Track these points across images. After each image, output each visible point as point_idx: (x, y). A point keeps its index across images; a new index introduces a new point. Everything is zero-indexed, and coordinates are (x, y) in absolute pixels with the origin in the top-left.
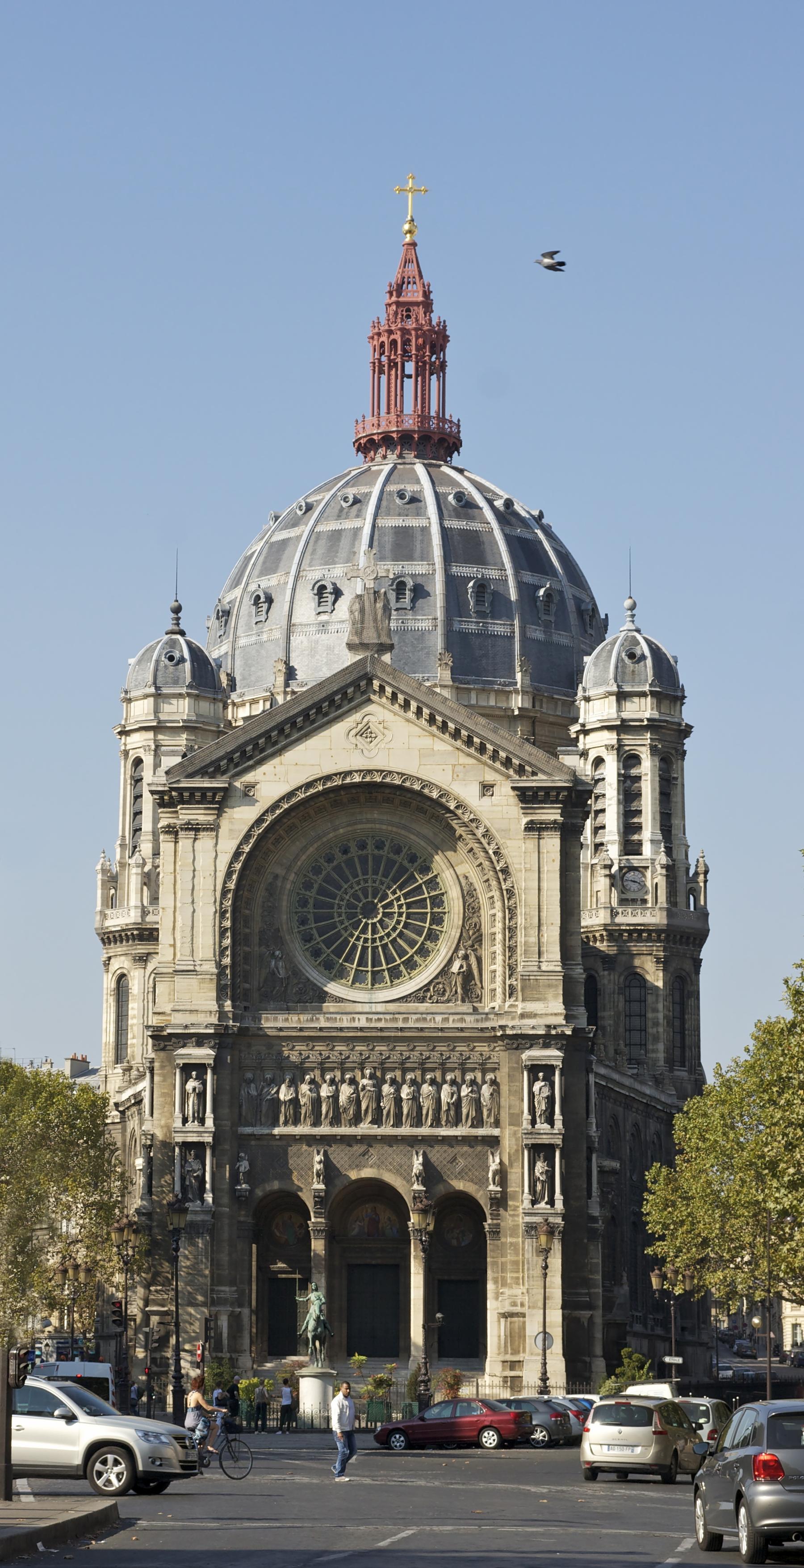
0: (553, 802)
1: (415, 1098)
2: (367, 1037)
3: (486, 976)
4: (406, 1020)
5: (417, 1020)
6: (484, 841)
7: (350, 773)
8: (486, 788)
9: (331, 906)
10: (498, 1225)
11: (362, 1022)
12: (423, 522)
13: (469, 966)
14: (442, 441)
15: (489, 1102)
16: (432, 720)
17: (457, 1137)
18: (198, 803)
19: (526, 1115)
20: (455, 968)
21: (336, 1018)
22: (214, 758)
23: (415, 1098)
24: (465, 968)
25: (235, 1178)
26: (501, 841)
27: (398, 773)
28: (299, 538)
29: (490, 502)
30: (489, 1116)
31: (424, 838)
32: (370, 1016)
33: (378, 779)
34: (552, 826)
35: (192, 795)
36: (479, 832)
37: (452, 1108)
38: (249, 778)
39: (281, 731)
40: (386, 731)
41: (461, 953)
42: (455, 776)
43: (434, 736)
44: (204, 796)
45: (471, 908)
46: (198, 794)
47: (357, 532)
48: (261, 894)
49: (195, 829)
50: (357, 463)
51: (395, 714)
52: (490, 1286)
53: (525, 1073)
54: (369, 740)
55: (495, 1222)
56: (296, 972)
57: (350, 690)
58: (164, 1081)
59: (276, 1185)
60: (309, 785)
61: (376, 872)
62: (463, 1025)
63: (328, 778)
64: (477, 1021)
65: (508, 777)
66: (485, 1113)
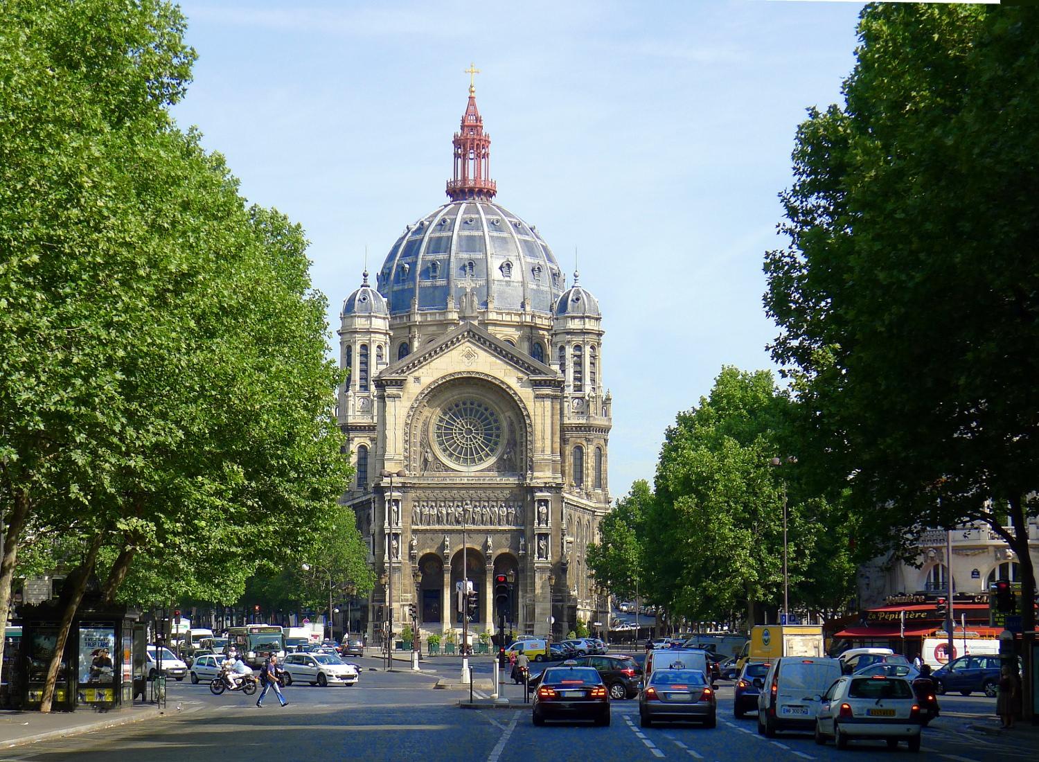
2: (467, 488)
3: (518, 461)
4: (484, 480)
7: (460, 373)
8: (520, 379)
9: (452, 430)
11: (466, 481)
12: (481, 234)
14: (488, 191)
16: (495, 350)
19: (536, 521)
20: (505, 457)
25: (411, 547)
28: (422, 240)
29: (511, 222)
31: (493, 401)
35: (391, 382)
38: (416, 374)
42: (505, 374)
43: (496, 357)
44: (396, 383)
45: (512, 431)
47: (450, 239)
48: (420, 425)
49: (395, 397)
50: (448, 199)
51: (479, 347)
52: (520, 593)
53: (536, 503)
56: (436, 458)
57: (460, 337)
59: (428, 551)
60: (443, 378)
61: (471, 415)
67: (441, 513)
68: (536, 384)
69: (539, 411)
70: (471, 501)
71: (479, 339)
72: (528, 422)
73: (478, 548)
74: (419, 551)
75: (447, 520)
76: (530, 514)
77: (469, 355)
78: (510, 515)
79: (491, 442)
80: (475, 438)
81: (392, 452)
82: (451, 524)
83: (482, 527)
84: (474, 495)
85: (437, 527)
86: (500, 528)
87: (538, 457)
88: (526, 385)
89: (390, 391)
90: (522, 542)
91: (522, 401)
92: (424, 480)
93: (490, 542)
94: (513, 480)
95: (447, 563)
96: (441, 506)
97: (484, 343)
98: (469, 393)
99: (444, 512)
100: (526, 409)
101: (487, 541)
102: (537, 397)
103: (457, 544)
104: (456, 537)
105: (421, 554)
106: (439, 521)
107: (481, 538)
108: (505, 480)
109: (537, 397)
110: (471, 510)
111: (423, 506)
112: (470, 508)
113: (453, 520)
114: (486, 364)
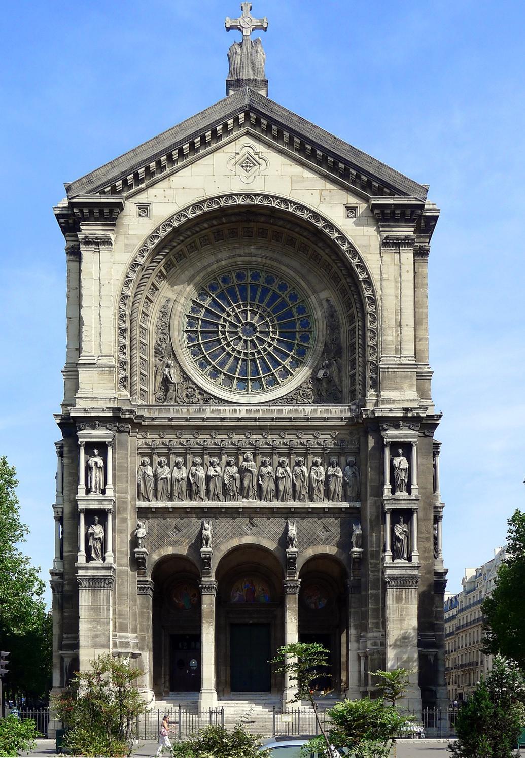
0: (407, 221)
4: (280, 411)
5: (290, 411)
6: (349, 255)
7: (230, 196)
8: (351, 210)
10: (359, 581)
11: (242, 412)
16: (302, 150)
17: (324, 508)
18: (97, 219)
21: (220, 410)
22: (109, 177)
26: (362, 255)
27: (273, 197)
32: (249, 408)
33: (257, 202)
34: (406, 242)
36: (345, 247)
38: (142, 198)
39: (170, 157)
40: (262, 161)
42: (322, 200)
43: (303, 165)
46: (96, 210)
51: (269, 145)
54: (248, 169)
55: (356, 578)
57: (230, 122)
58: (71, 463)
59: (170, 550)
60: (197, 206)
62: (330, 415)
63: (212, 200)
64: (341, 412)
65: (367, 200)
67: (194, 476)
68: (383, 217)
69: (391, 271)
70: (254, 454)
71: (269, 127)
72: (367, 293)
73: (272, 546)
74: (152, 550)
75: (208, 491)
76: (371, 474)
77: (248, 163)
78: (332, 480)
79: (295, 337)
80: (262, 341)
81: (95, 352)
82: (216, 497)
83: (276, 504)
84: (261, 443)
85: (187, 504)
86: (313, 505)
87: (388, 359)
88: (364, 220)
89: (88, 230)
90: (358, 531)
91: (355, 253)
92: (160, 411)
93: (293, 530)
94: (337, 412)
95: (208, 574)
96: (194, 464)
97: (279, 137)
98: (251, 254)
99: (201, 473)
100: (364, 268)
101: (286, 530)
102: (386, 243)
103: (227, 538)
104: (225, 524)
105: (156, 557)
106: (191, 490)
107: (274, 527)
108: (321, 411)
109: (386, 243)
110: (255, 471)
111: (160, 464)
112: (252, 465)
113: (219, 490)
114: (282, 179)
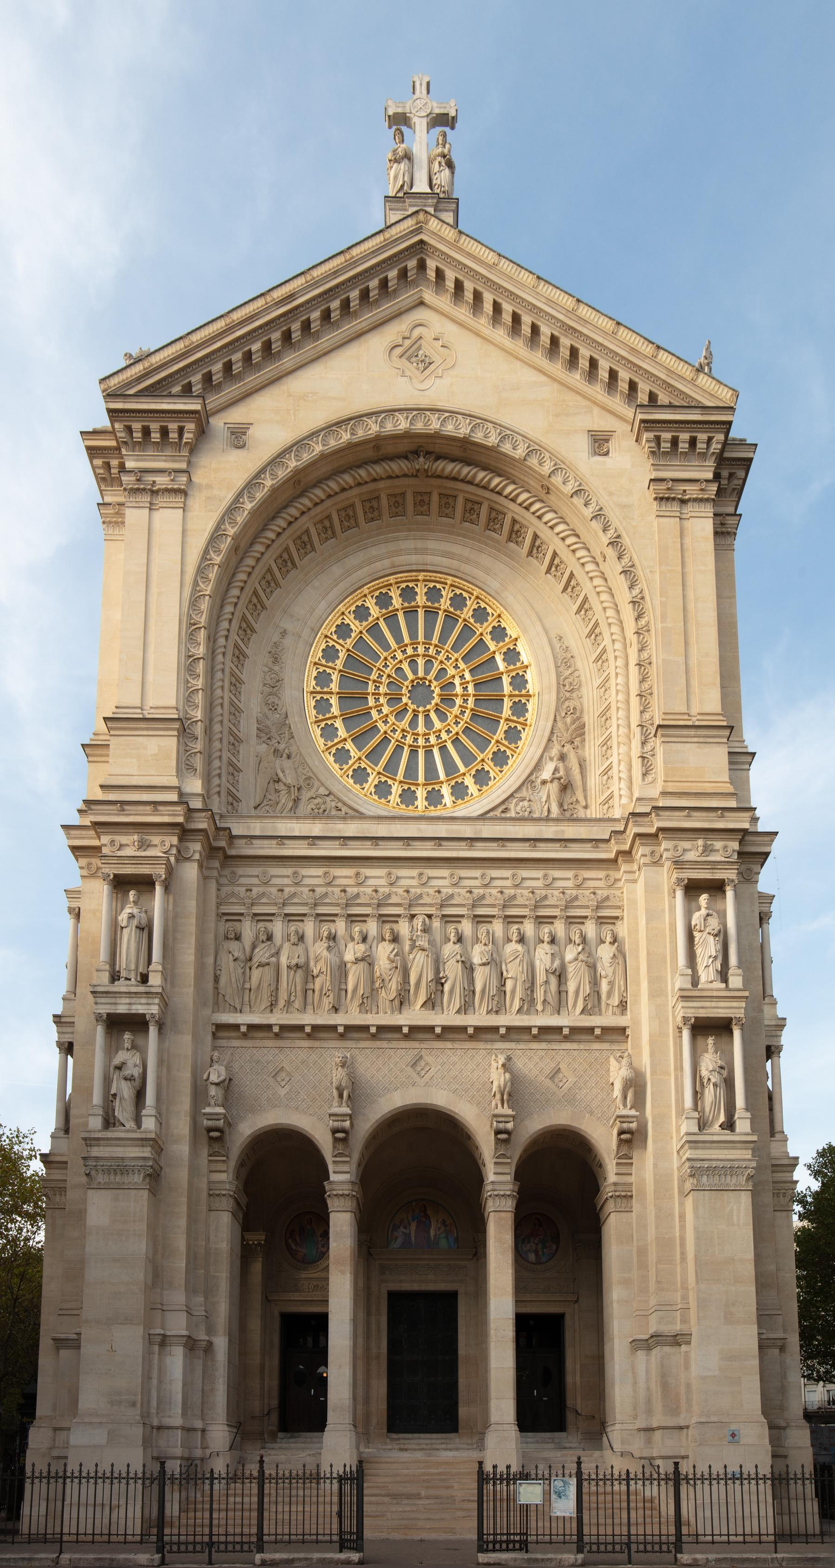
1: (494, 962)
13: (567, 770)
15: (610, 971)
23: (494, 962)
24: (562, 773)
30: (610, 994)
37: (553, 981)
41: (555, 752)
66: (604, 987)
